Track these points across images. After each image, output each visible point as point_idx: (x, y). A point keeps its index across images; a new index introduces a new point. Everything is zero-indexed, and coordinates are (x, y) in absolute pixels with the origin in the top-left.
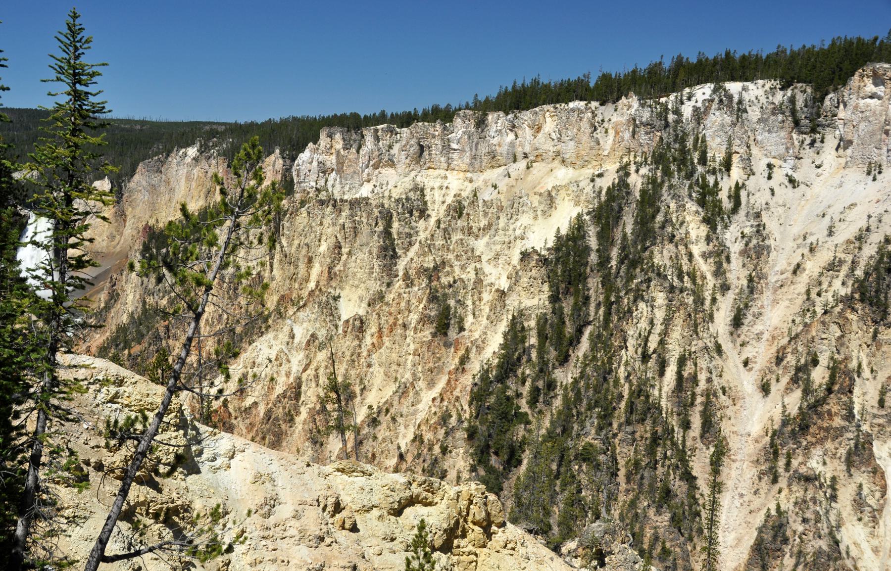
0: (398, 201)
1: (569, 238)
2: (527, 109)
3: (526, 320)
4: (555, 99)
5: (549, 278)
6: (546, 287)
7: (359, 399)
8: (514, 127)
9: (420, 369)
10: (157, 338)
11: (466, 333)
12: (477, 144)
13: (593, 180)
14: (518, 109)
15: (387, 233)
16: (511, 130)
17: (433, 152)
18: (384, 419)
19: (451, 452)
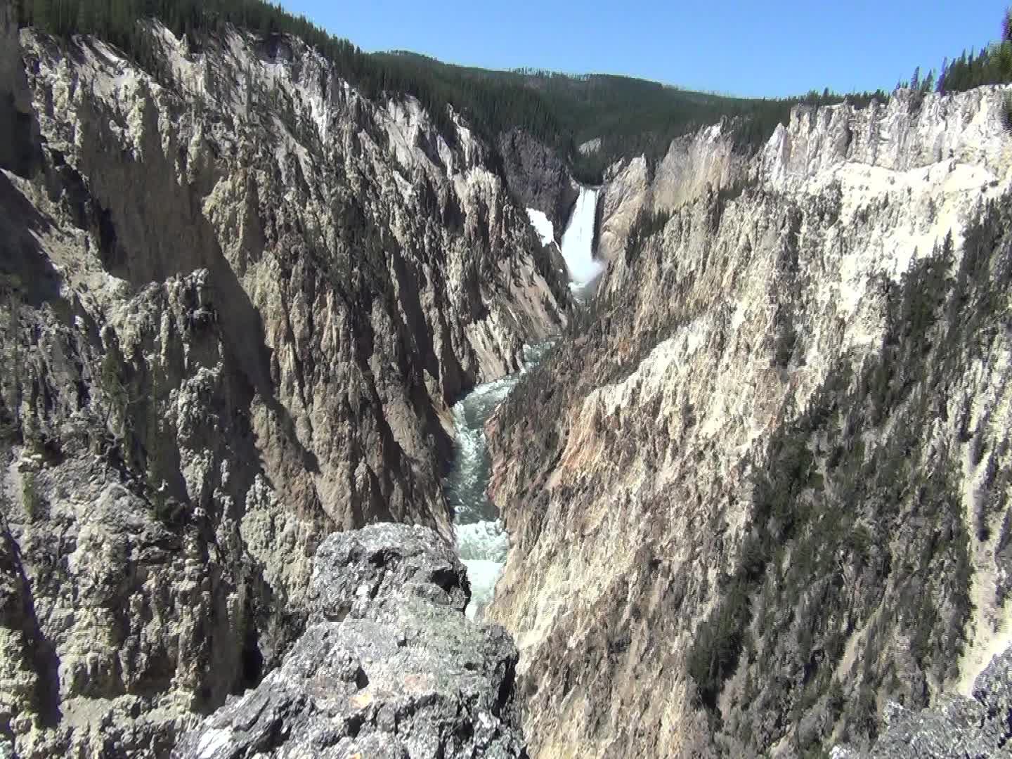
0: (813, 199)
1: (928, 263)
2: (964, 90)
3: (855, 361)
4: (998, 79)
5: (889, 311)
6: (883, 322)
7: (697, 426)
8: (946, 113)
9: (753, 403)
10: (599, 331)
11: (805, 368)
12: (906, 134)
13: (984, 190)
14: (955, 89)
15: (792, 238)
16: (943, 118)
17: (861, 141)
18: (709, 454)
19: (737, 503)
